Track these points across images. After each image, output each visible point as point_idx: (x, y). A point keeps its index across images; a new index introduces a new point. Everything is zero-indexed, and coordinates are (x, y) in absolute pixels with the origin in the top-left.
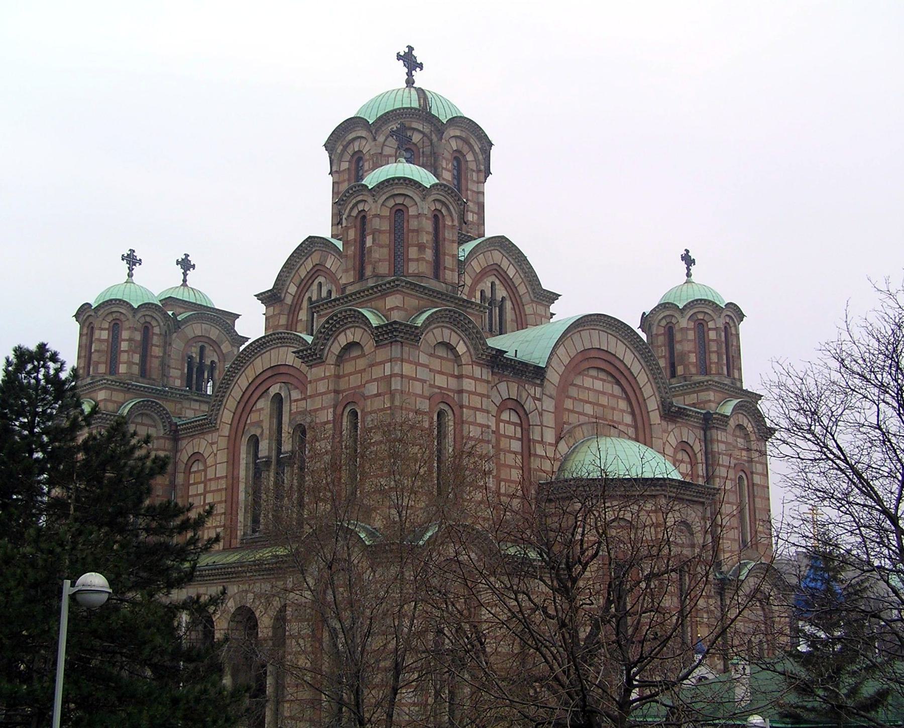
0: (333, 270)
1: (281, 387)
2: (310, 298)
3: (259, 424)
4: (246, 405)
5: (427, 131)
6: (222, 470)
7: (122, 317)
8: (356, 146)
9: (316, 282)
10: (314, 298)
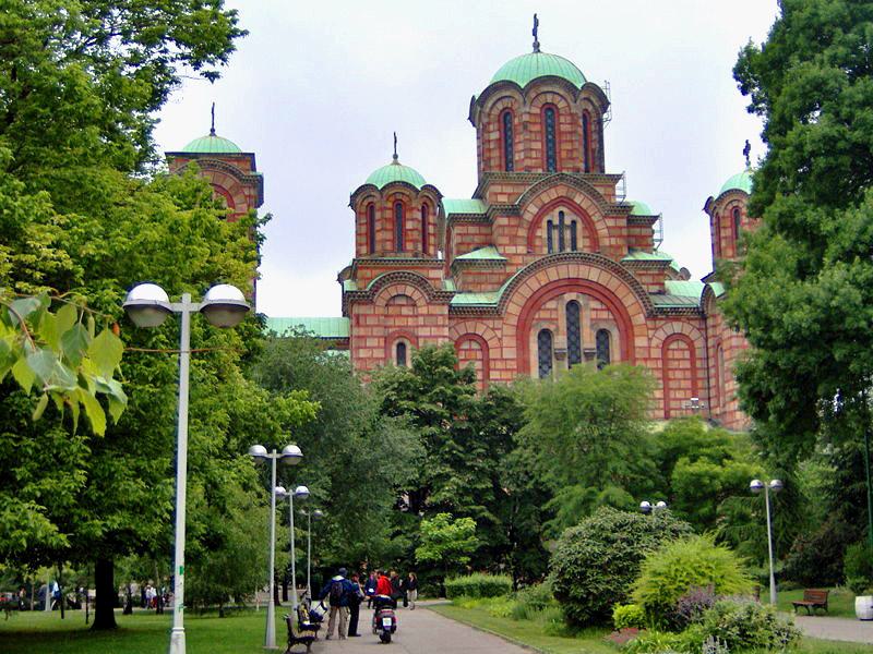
0: (584, 206)
1: (578, 297)
2: (550, 222)
3: (551, 320)
4: (535, 303)
5: (597, 104)
6: (510, 353)
7: (429, 204)
8: (549, 98)
9: (557, 210)
10: (556, 222)
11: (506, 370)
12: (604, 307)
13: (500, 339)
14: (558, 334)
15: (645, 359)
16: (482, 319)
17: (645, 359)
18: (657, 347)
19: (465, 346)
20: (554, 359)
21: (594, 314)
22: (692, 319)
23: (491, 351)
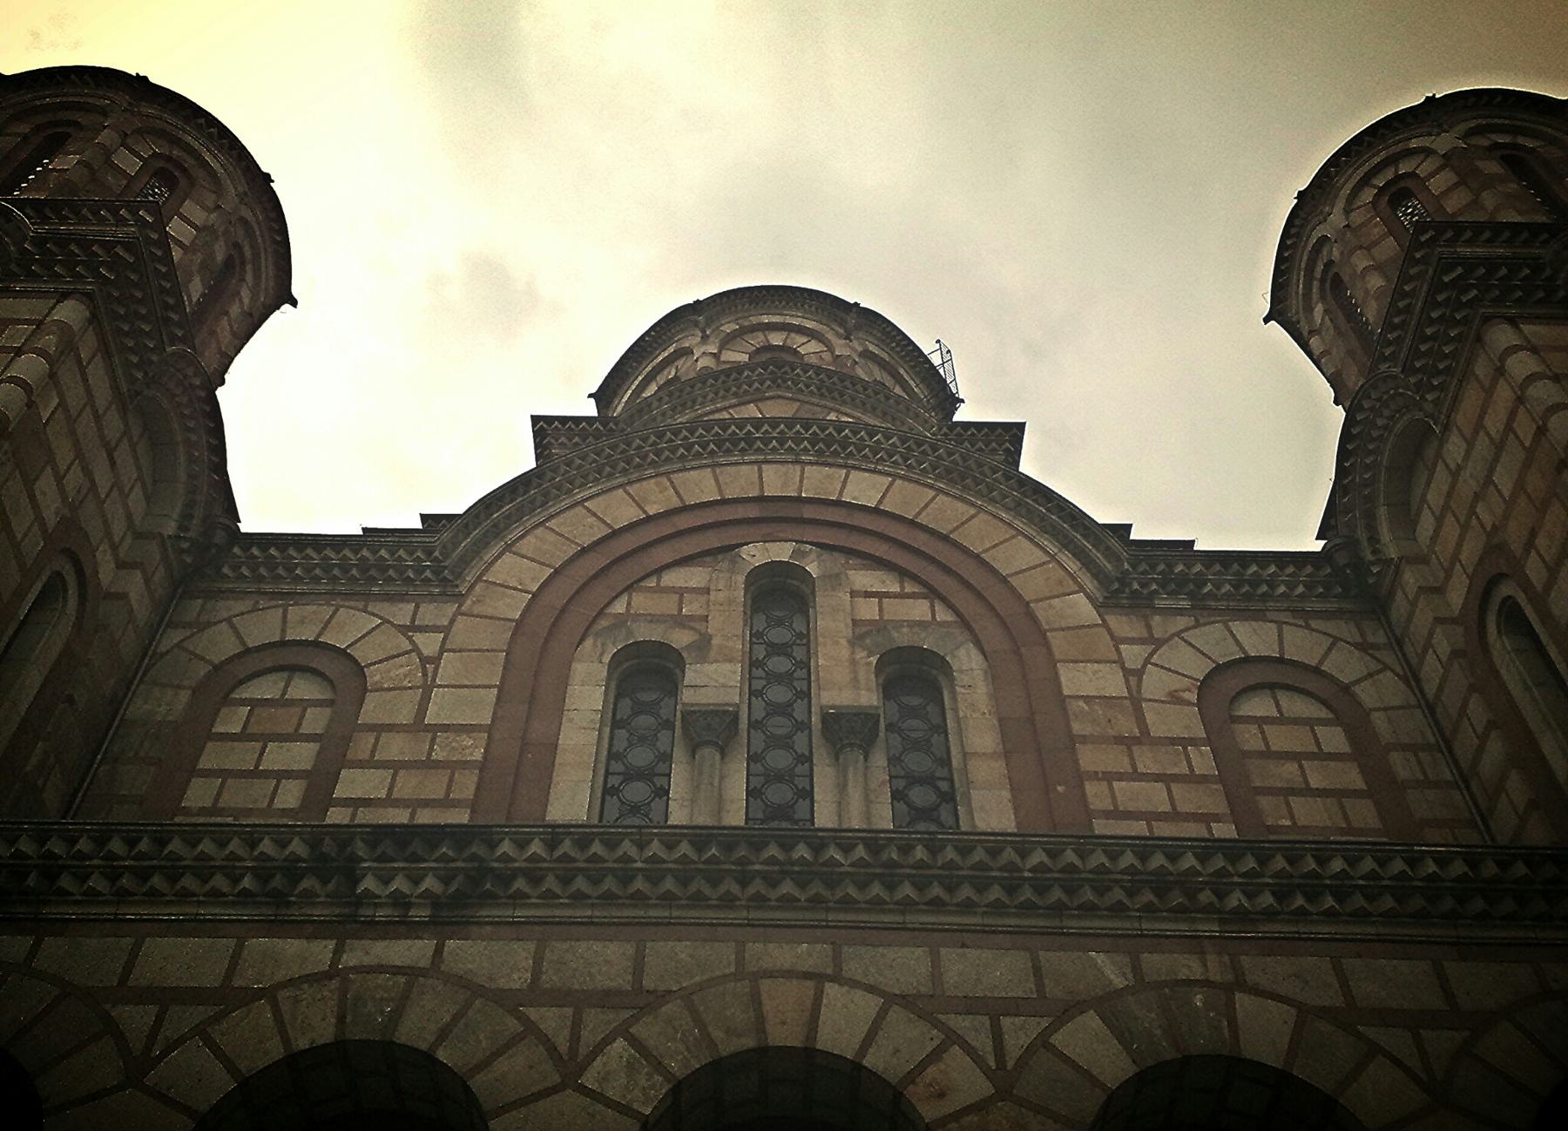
3: (680, 621)
11: (429, 765)
12: (910, 588)
13: (424, 660)
14: (703, 659)
15: (1126, 742)
16: (368, 597)
17: (1126, 742)
18: (1175, 698)
19: (265, 689)
20: (679, 754)
21: (868, 610)
22: (1318, 614)
23: (371, 701)
